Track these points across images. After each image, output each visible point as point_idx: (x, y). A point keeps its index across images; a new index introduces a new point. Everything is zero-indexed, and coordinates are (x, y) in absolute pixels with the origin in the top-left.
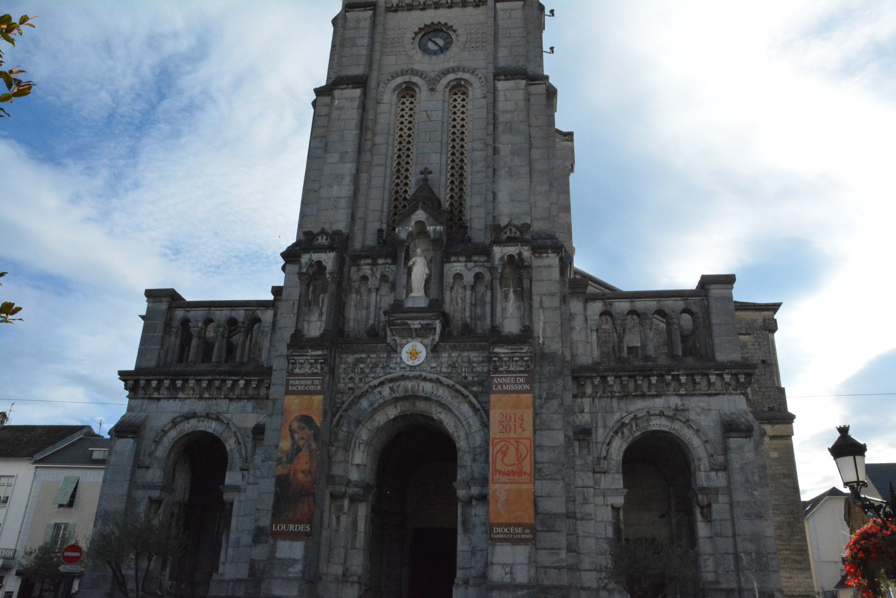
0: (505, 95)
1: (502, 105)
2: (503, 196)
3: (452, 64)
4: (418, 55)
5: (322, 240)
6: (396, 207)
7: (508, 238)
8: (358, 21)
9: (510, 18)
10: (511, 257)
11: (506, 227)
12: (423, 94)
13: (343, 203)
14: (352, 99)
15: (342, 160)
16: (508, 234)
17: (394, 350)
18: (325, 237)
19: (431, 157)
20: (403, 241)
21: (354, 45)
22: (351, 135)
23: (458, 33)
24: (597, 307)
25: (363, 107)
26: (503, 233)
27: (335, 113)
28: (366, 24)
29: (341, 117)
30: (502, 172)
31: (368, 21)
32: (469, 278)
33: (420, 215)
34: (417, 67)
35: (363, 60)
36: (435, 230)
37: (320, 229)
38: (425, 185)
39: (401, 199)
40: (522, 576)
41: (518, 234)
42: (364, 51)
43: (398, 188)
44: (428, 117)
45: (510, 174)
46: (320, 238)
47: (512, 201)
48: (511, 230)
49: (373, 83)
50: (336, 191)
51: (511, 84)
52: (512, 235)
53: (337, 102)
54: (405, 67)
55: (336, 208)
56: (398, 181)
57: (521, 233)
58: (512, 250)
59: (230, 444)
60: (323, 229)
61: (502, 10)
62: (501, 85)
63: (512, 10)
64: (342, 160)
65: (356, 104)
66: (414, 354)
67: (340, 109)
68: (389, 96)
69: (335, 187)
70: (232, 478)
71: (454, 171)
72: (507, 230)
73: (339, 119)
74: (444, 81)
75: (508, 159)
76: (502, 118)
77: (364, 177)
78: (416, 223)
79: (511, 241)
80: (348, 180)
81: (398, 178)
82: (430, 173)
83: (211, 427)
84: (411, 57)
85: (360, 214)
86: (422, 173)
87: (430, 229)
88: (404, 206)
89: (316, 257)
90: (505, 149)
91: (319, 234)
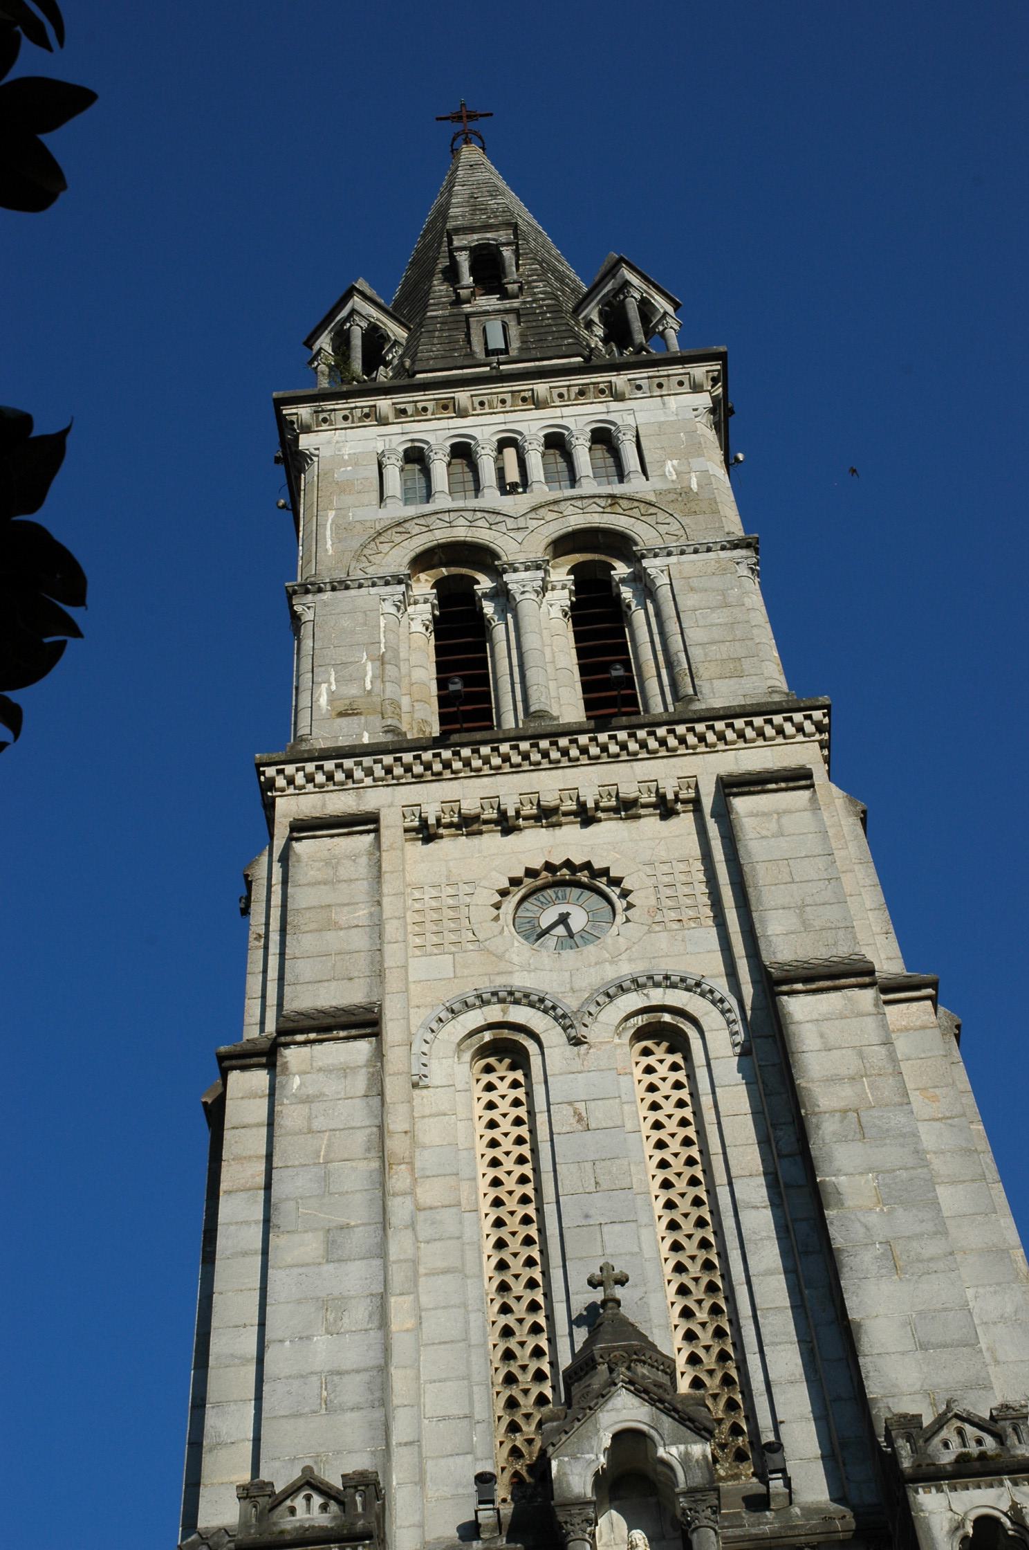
0: (822, 1036)
3: (626, 969)
4: (518, 949)
6: (512, 1404)
7: (962, 1459)
8: (332, 862)
9: (780, 834)
10: (986, 1524)
11: (941, 1422)
13: (353, 1390)
14: (345, 1071)
15: (333, 1251)
16: (956, 1448)
18: (317, 1500)
20: (583, 1503)
22: (355, 1175)
23: (626, 884)
26: (937, 1441)
29: (316, 1125)
31: (364, 860)
33: (624, 1410)
34: (521, 981)
35: (361, 964)
36: (686, 1459)
37: (296, 1474)
39: (525, 1379)
41: (990, 1443)
42: (360, 940)
43: (512, 1344)
44: (580, 1120)
45: (893, 1263)
46: (299, 1502)
47: (923, 1347)
48: (960, 1432)
49: (392, 1030)
50: (323, 1350)
51: (832, 1001)
52: (973, 1449)
53: (297, 1081)
54: (485, 985)
55: (330, 1407)
56: (509, 1320)
57: (1000, 1438)
60: (307, 1470)
61: (751, 815)
63: (780, 814)
64: (333, 1251)
65: (360, 1083)
67: (308, 1100)
69: (321, 1342)
71: (685, 1279)
72: (948, 1433)
73: (310, 1131)
74: (634, 1001)
75: (873, 1219)
77: (400, 1308)
78: (616, 1437)
79: (971, 1470)
80: (360, 1313)
81: (505, 1309)
82: (622, 1281)
84: (500, 957)
85: (400, 1432)
86: (593, 1283)
87: (670, 1452)
88: (542, 1400)
91: (292, 1491)
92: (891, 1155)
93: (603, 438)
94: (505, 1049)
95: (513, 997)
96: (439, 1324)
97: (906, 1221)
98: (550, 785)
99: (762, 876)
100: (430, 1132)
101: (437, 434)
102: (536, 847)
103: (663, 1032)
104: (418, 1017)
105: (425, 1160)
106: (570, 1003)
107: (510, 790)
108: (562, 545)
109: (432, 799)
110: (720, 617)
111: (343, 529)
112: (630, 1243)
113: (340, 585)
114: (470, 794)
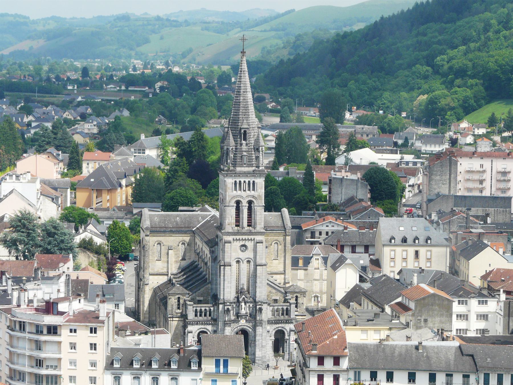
3: (247, 257)
5: (228, 304)
22: (229, 277)
24: (272, 307)
28: (230, 247)
34: (240, 257)
40: (260, 356)
42: (230, 254)
58: (260, 306)
68: (234, 264)
76: (258, 275)
92: (261, 280)
93: (254, 182)
94: (238, 262)
95: (239, 258)
97: (261, 285)
98: (244, 237)
99: (258, 252)
102: (242, 243)
103: (249, 262)
107: (241, 237)
109: (235, 237)
110: (260, 216)
111: (229, 196)
112: (244, 281)
113: (228, 206)
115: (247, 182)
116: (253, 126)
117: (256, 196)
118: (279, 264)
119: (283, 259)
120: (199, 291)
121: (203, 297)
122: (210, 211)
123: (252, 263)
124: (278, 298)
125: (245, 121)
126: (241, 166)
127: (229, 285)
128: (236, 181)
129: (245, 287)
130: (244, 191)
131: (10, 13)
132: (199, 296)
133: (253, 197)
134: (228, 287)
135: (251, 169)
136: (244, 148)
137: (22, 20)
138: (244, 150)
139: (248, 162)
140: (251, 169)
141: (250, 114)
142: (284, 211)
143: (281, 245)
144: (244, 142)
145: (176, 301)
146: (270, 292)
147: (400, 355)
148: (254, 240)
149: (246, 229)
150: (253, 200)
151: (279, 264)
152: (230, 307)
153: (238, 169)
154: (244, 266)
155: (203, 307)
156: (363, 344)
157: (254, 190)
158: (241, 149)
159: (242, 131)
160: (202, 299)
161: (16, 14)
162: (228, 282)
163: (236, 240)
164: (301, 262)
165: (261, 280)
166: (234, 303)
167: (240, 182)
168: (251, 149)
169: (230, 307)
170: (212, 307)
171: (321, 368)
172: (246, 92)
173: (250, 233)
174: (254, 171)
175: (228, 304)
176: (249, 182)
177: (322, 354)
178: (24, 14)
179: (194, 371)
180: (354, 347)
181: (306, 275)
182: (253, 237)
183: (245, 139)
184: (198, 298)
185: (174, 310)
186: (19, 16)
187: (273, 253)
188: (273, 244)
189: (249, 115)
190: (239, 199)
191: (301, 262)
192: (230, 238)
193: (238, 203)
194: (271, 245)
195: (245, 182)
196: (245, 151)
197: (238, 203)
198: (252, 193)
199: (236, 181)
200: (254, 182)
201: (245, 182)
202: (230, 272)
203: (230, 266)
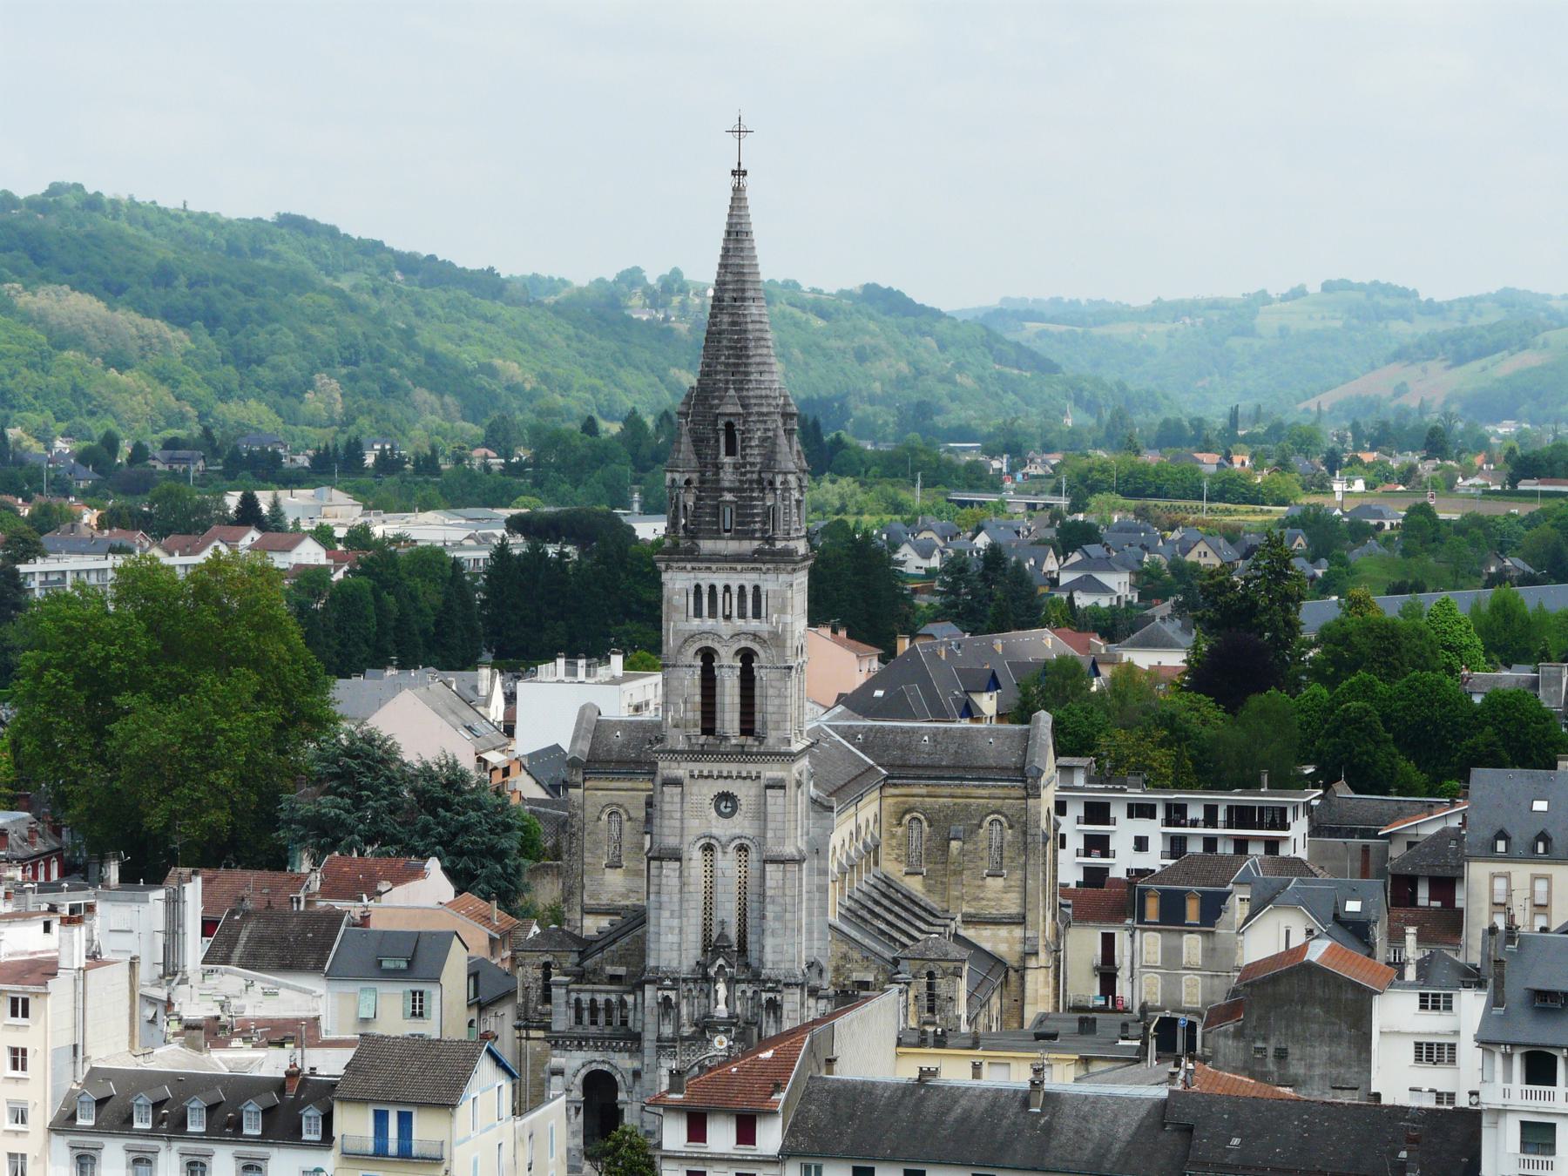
1: (769, 883)
2: (768, 949)
3: (738, 831)
5: (668, 982)
12: (719, 855)
13: (675, 947)
17: (709, 1041)
19: (728, 911)
21: (672, 818)
22: (676, 898)
25: (681, 875)
27: (664, 881)
28: (677, 799)
30: (768, 933)
32: (749, 994)
33: (721, 961)
34: (715, 832)
38: (722, 936)
42: (677, 824)
45: (773, 934)
58: (771, 995)
59: (618, 1077)
62: (769, 867)
64: (672, 916)
66: (721, 1043)
68: (697, 854)
70: (621, 1096)
76: (769, 893)
79: (771, 990)
83: (606, 1068)
89: (666, 993)
90: (769, 915)
92: (778, 909)
93: (757, 588)
94: (708, 848)
95: (711, 837)
96: (693, 921)
97: (777, 925)
98: (726, 768)
100: (693, 872)
101: (705, 579)
103: (742, 848)
104: (691, 838)
105: (692, 880)
106: (724, 840)
107: (715, 768)
108: (737, 653)
109: (697, 768)
110: (777, 702)
114: (706, 768)
115: (735, 589)
116: (765, 410)
117: (766, 636)
118: (1007, 889)
119: (1019, 874)
120: (613, 948)
121: (627, 965)
122: (835, 728)
123: (753, 855)
124: (871, 978)
125: (732, 392)
126: (716, 535)
127: (676, 922)
128: (698, 587)
129: (733, 933)
130: (728, 618)
131: (1355, 280)
132: (613, 964)
133: (755, 636)
134: (671, 928)
135: (748, 546)
136: (728, 477)
137: (1391, 303)
138: (727, 484)
139: (739, 524)
140: (748, 546)
141: (752, 369)
142: (1038, 719)
143: (1011, 827)
144: (727, 460)
145: (539, 973)
146: (845, 957)
147: (965, 1118)
148: (758, 777)
149: (734, 741)
150: (756, 647)
151: (1007, 889)
152: (672, 995)
153: (707, 545)
154: (727, 863)
155: (600, 991)
156: (864, 1083)
157: (757, 615)
158: (718, 481)
159: (721, 424)
160: (621, 971)
161: (1375, 283)
162: (672, 912)
163: (701, 776)
164: (1192, 910)
165: (778, 909)
166: (695, 981)
167: (712, 588)
168: (751, 482)
169: (672, 995)
170: (629, 993)
171: (696, 1148)
172: (743, 299)
173: (742, 754)
174: (755, 552)
175: (668, 982)
176: (742, 588)
177: (697, 1103)
178: (1399, 282)
179: (310, 1145)
180: (829, 1092)
181: (1209, 953)
182: (753, 768)
183: (731, 451)
184: (610, 970)
185: (532, 1005)
186: (1388, 290)
187: (985, 854)
188: (986, 824)
189: (747, 374)
190: (710, 643)
191: (1192, 910)
192: (681, 770)
193: (708, 656)
194: (980, 826)
195: (727, 588)
196: (730, 490)
197: (708, 656)
198: (753, 625)
199: (698, 587)
200: (757, 588)
201: (727, 588)
202: (675, 881)
203: (679, 859)
